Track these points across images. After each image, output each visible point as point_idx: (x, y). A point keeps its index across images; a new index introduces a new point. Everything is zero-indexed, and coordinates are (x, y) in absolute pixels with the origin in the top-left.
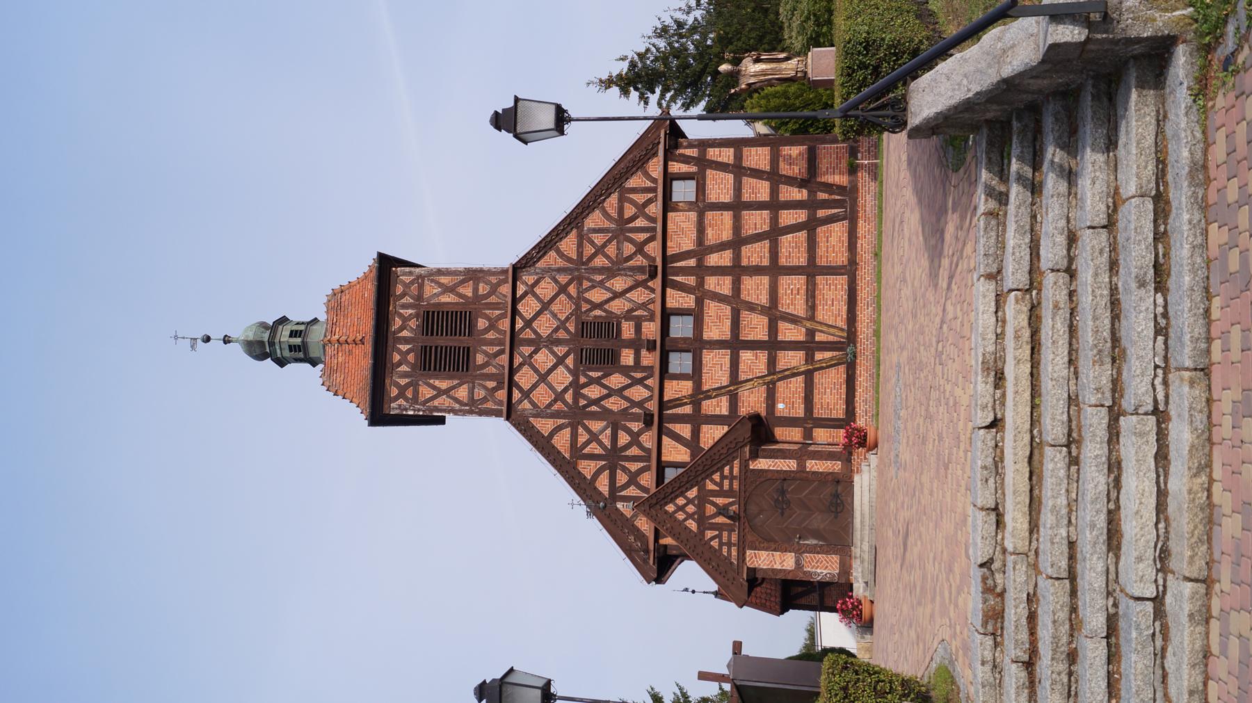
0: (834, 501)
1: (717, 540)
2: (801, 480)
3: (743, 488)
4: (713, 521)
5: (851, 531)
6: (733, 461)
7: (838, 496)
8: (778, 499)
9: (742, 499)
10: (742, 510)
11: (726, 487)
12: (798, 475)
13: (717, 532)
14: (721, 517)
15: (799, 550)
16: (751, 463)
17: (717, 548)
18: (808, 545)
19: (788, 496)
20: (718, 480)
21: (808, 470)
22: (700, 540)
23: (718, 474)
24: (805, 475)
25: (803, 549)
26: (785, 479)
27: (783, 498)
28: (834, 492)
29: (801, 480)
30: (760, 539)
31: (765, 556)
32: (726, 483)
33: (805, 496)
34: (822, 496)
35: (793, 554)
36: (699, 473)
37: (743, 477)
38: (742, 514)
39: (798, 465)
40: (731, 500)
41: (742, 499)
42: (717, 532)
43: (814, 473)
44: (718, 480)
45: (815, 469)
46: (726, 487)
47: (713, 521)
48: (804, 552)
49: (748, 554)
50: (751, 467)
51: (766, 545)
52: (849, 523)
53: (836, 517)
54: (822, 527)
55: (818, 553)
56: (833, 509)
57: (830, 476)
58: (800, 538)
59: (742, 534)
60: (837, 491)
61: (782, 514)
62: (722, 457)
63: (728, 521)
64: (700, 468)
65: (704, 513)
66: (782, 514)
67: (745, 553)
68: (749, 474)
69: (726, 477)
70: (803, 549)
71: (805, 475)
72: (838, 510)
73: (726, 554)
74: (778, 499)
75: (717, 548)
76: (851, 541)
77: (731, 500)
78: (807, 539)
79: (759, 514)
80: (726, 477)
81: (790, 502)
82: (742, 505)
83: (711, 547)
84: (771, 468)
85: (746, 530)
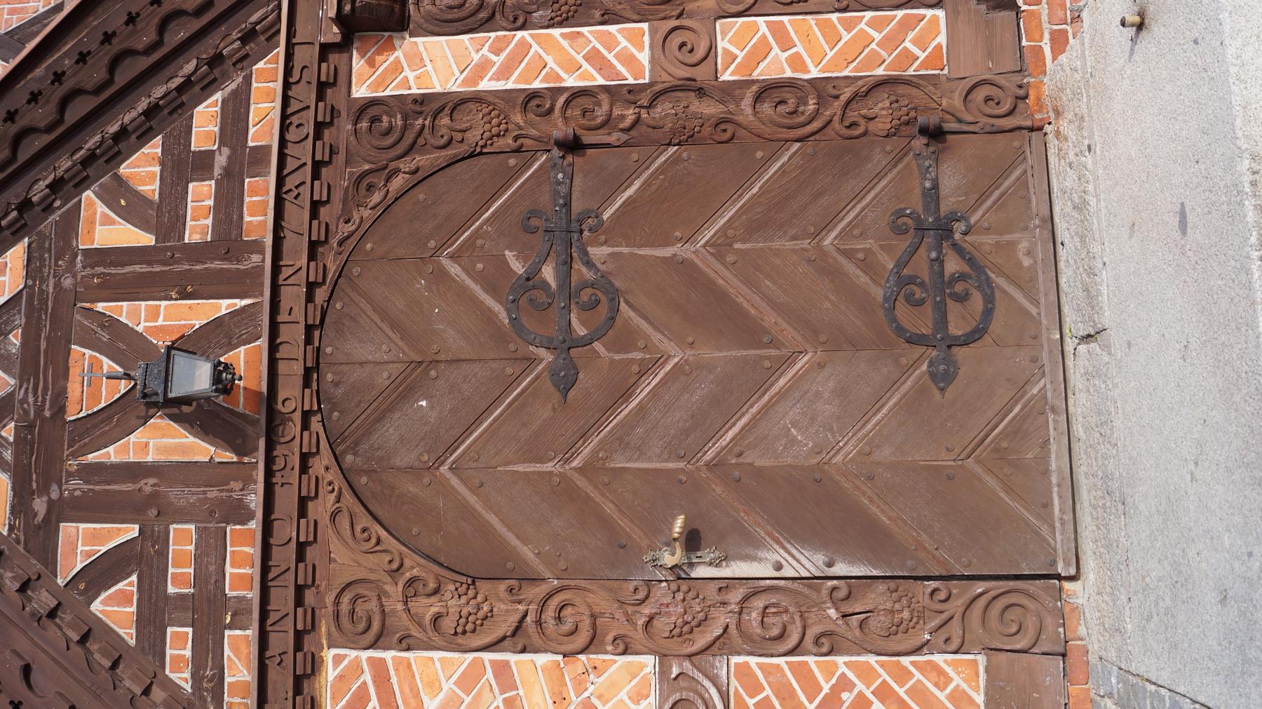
0: (921, 266)
1: (130, 584)
2: (685, 137)
3: (297, 216)
4: (111, 454)
5: (1056, 463)
6: (245, 61)
7: (944, 230)
8: (531, 277)
9: (293, 296)
10: (291, 371)
11: (198, 228)
12: (663, 109)
13: (133, 531)
14: (159, 422)
15: (685, 631)
16: (358, 63)
17: (129, 634)
18: (755, 588)
19: (598, 252)
20: (151, 189)
21: (726, 76)
22: (23, 588)
23: (154, 148)
24: (709, 109)
25: (722, 619)
26: (573, 146)
27: (567, 264)
28: (915, 203)
29: (685, 137)
30: (415, 567)
31: (448, 686)
32: (201, 194)
33: (719, 247)
34: (828, 240)
35: (649, 662)
36: (38, 142)
37: (302, 153)
38: (291, 395)
39: (661, 44)
40: (225, 306)
41: (293, 296)
42: (133, 531)
43: (769, 90)
44: (151, 189)
45: (776, 66)
46: (198, 228)
47: (111, 454)
48: (720, 645)
49: (330, 673)
50: (360, 91)
51: (453, 604)
52: (1039, 408)
53: (943, 377)
54: (848, 449)
55: (830, 644)
56: (922, 323)
57: (880, 105)
58: (692, 541)
59: (286, 531)
60: (933, 195)
61: (565, 381)
62: (178, 34)
63: (199, 449)
64: (41, 115)
65: (60, 409)
66: (565, 381)
67: (315, 665)
68: (346, 125)
69: (202, 165)
70: (722, 619)
71: (709, 109)
72: (956, 328)
73: (182, 678)
74: (531, 277)
75: (129, 634)
76: (1060, 541)
77: (225, 306)
78: (749, 545)
79: (404, 390)
80: (202, 165)
81: (614, 296)
82: (293, 334)
83: (90, 632)
84: (486, 85)
85: (320, 509)
